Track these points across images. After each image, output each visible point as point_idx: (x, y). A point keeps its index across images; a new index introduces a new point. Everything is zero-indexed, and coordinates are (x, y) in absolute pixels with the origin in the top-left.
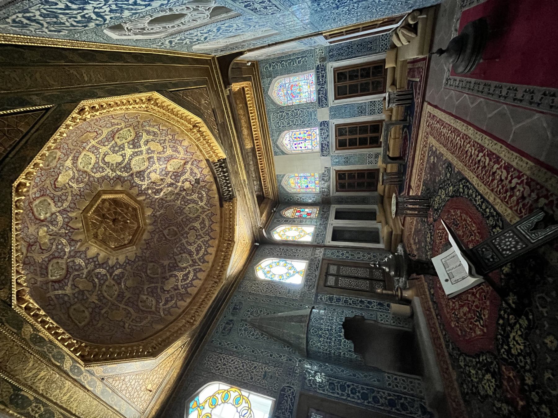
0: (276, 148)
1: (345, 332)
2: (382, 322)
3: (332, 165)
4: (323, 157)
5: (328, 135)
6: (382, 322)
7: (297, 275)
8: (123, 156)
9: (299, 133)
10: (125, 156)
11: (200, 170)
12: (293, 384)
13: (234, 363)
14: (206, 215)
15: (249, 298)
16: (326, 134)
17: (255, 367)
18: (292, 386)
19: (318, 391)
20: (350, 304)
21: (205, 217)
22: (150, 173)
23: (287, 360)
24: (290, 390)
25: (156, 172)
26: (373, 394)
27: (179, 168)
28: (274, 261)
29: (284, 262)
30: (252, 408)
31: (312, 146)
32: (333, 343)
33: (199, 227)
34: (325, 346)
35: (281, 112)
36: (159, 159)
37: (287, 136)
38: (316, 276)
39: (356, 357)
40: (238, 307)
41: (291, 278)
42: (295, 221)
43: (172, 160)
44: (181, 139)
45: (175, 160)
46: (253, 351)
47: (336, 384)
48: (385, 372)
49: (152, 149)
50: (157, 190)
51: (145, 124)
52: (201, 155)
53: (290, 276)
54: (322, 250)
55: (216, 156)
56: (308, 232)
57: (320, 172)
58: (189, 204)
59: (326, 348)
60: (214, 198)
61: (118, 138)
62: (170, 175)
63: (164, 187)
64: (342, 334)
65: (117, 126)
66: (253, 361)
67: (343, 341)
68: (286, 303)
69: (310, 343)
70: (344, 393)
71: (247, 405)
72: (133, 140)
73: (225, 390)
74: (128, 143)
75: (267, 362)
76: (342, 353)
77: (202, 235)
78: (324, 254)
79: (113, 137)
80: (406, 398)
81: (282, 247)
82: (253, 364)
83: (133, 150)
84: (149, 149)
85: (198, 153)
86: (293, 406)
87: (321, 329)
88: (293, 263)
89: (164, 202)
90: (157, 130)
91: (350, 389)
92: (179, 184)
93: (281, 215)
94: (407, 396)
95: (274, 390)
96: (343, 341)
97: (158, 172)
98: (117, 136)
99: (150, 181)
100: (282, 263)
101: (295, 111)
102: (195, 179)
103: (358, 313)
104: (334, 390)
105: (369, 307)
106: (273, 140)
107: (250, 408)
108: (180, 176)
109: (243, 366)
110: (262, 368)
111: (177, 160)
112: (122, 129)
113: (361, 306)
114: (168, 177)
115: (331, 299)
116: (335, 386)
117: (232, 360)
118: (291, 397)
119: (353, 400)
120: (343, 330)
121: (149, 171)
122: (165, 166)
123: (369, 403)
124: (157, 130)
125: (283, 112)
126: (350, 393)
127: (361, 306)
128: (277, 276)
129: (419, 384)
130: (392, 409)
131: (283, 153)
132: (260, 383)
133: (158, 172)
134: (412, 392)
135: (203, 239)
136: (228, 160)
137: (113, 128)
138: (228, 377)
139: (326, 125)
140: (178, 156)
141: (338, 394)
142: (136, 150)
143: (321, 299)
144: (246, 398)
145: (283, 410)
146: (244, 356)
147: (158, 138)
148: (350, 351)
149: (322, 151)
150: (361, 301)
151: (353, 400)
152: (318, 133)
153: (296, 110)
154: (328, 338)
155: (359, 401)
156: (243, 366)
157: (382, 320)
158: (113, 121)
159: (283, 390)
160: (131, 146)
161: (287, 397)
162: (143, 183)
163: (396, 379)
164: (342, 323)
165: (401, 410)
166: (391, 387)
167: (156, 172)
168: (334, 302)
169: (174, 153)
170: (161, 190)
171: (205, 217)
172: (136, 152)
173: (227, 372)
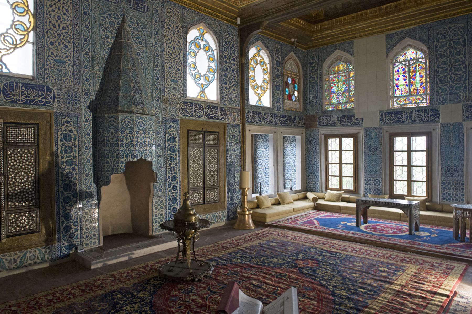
0: (399, 37)
1: (133, 162)
3: (366, 129)
4: (379, 115)
5: (414, 121)
7: (198, 89)
9: (423, 74)
12: (58, 101)
13: (64, 14)
15: (156, 21)
16: (417, 119)
17: (66, 47)
18: (56, 100)
19: (59, 134)
20: (170, 164)
23: (85, 90)
24: (51, 98)
28: (215, 52)
29: (214, 67)
30: (17, 50)
31: (399, 97)
35: (464, 41)
37: (420, 55)
38: (199, 117)
40: (141, 6)
41: (193, 81)
42: (278, 77)
46: (85, 40)
47: (72, 154)
53: (197, 77)
54: (238, 122)
56: (262, 99)
57: (355, 111)
59: (111, 140)
66: (73, 42)
67: (123, 160)
68: (158, 78)
70: (65, 164)
71: (18, 42)
73: (28, 6)
75: (77, 63)
76: (108, 160)
78: (232, 125)
80: (76, 230)
81: (237, 62)
82: (69, 42)
86: (34, 104)
87: (131, 132)
88: (215, 82)
91: (71, 171)
93: (287, 54)
94: (79, 231)
95: (46, 77)
96: (123, 160)
100: (213, 65)
101: (462, 67)
103: (160, 175)
104: (66, 153)
105: (169, 187)
106: (414, 30)
107: (16, 47)
109: (64, 28)
110: (67, 57)
113: (169, 177)
115: (173, 139)
116: (69, 153)
117: (67, 11)
118: (44, 100)
120: (135, 160)
123: (62, 192)
125: (464, 46)
128: (194, 60)
130: (62, 216)
131: (389, 50)
132: (49, 56)
134: (85, 236)
138: (45, 8)
139: (432, 118)
141: (62, 158)
143: (171, 127)
144: (26, 39)
145: (26, 92)
146: (77, 28)
149: (388, 113)
150: (175, 178)
152: (420, 105)
153: (465, 68)
154: (122, 141)
155: (61, 182)
156: (64, 28)
159: (49, 90)
161: (43, 95)
164: (143, 158)
165: (64, 226)
168: (169, 145)
173: (51, 6)
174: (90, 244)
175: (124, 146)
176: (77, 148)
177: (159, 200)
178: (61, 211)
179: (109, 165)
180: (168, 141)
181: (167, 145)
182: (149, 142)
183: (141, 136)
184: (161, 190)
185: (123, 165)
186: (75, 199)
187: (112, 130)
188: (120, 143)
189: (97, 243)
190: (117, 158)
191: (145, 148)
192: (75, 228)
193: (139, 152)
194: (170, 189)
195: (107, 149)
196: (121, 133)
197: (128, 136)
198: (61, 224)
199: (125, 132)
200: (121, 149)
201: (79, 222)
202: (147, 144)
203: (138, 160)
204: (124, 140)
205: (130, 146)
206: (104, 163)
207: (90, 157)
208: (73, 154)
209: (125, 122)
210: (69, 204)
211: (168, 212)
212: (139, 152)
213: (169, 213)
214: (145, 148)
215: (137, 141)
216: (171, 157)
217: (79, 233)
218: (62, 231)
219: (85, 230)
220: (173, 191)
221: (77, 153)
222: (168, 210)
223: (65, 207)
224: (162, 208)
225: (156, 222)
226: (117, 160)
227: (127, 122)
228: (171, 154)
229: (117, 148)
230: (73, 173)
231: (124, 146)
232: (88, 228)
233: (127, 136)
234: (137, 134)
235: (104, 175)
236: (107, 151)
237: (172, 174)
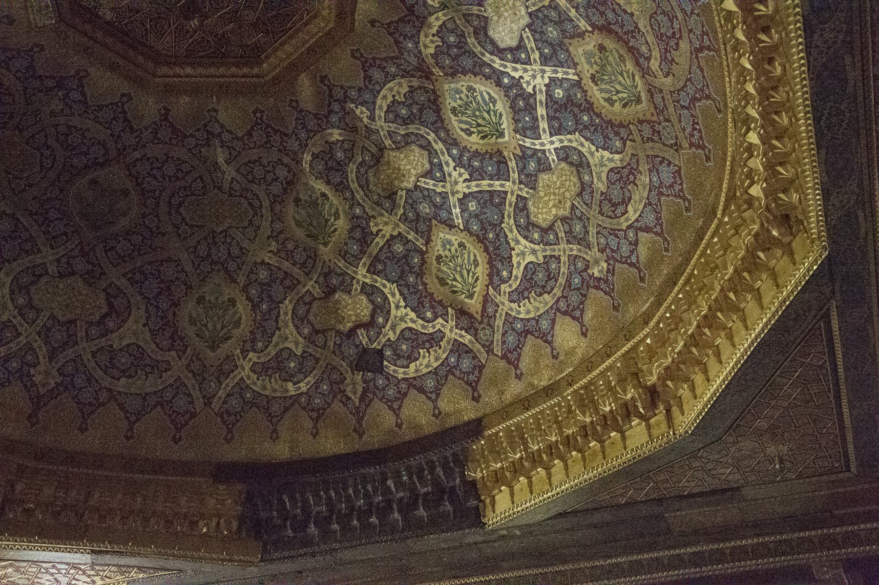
8: (516, 53)
10: (516, 61)
11: (430, 384)
14: (178, 386)
21: (169, 377)
22: (427, 147)
25: (428, 174)
27: (442, 282)
33: (115, 341)
36: (495, 200)
43: (482, 258)
44: (588, 315)
45: (481, 271)
49: (544, 178)
50: (340, 168)
51: (666, 175)
52: (508, 397)
55: (498, 479)
58: (255, 307)
60: (274, 436)
61: (602, 48)
62: (411, 236)
63: (354, 203)
65: (656, 54)
72: (590, 107)
74: (578, 84)
77: (70, 353)
79: (606, 29)
83: (541, 97)
84: (544, 166)
85: (515, 389)
89: (276, 189)
90: (632, 215)
92: (362, 271)
97: (430, 184)
98: (610, 44)
99: (388, 142)
102: (380, 353)
108: (400, 281)
111: (483, 279)
112: (645, 72)
114: (402, 228)
121: (439, 146)
122: (459, 221)
124: (632, 215)
133: (430, 184)
135: (42, 352)
136: (472, 536)
137: (651, 39)
140: (504, 287)
142: (541, 111)
147: (594, 212)
158: (684, 45)
160: (559, 93)
162: (380, 113)
167: (428, 174)
169: (518, 272)
170: (341, 187)
171: (169, 377)
172: (531, 108)
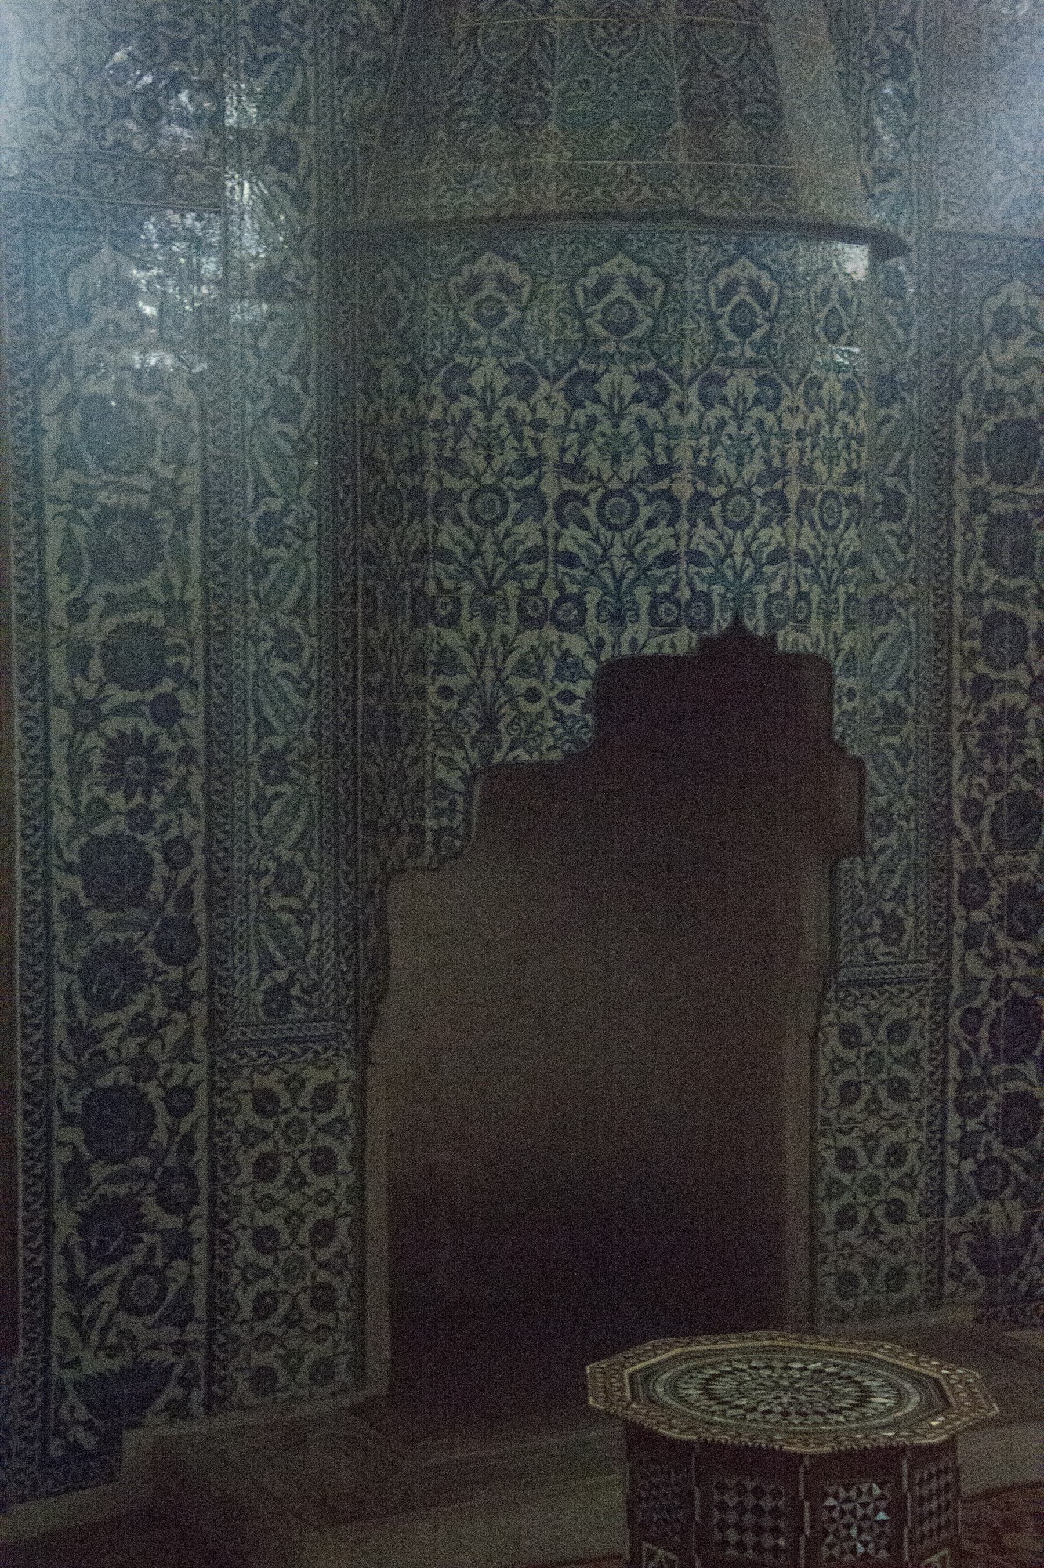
2: (833, 1045)
6: (833, 1045)
20: (981, 688)
26: (152, 1210)
32: (529, 532)
34: (488, 445)
39: (441, 788)
47: (151, 582)
48: (364, 1063)
64: (639, 629)
67: (575, 644)
69: (490, 264)
76: (451, 638)
91: (147, 729)
94: (200, 1252)
96: (575, 644)
105: (970, 904)
113: (973, 810)
119: (59, 767)
123: (74, 912)
126: (111, 727)
127: (973, 810)
129: (323, 1370)
130: (69, 1119)
148: (489, 722)
151: (59, 767)
154: (574, 470)
155: (62, 821)
157: (849, 1035)
163: (324, 1163)
164: (757, 624)
166: (247, 1115)
168: (980, 501)
174: (283, 1377)
175: (590, 513)
176: (194, 528)
177: (873, 1019)
178: (60, 1069)
179: (458, 682)
180: (973, 470)
181: (963, 505)
182: (807, 474)
183: (740, 419)
184: (893, 926)
185: (582, 687)
186: (175, 974)
187: (490, 362)
188: (550, 489)
189: (343, 1375)
190: (527, 622)
191: (772, 536)
192: (172, 1222)
193: (719, 576)
194: (979, 916)
195: (444, 540)
196: (568, 392)
197: (627, 426)
198: (58, 1183)
199: (603, 388)
200: (566, 544)
201: (202, 1174)
202: (793, 494)
203: (704, 643)
204: (594, 463)
205: (646, 512)
206: (419, 665)
207: (299, 609)
208: (166, 586)
209: (604, 286)
210: (124, 1017)
211: (954, 1134)
212: (719, 576)
213: (966, 1149)
214: (772, 536)
215: (706, 473)
216: (994, 620)
217: (201, 1271)
218: (67, 1251)
219: (247, 1250)
220: (1004, 941)
221: (195, 575)
222: (954, 1119)
223: (95, 1037)
224: (899, 1090)
225: (845, 1219)
226: (529, 639)
227: (620, 290)
228: (998, 591)
229: (529, 532)
230: (165, 744)
231: (590, 513)
232: (272, 1233)
233: (616, 418)
234: (707, 404)
235: (414, 775)
236: (444, 555)
237: (997, 780)
